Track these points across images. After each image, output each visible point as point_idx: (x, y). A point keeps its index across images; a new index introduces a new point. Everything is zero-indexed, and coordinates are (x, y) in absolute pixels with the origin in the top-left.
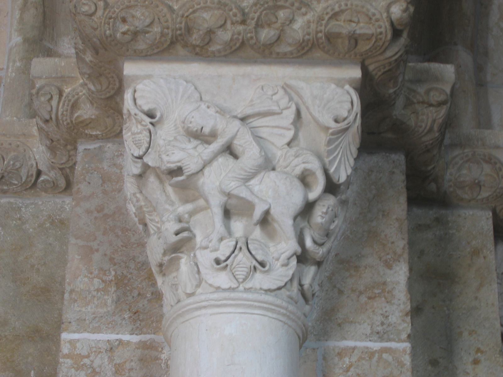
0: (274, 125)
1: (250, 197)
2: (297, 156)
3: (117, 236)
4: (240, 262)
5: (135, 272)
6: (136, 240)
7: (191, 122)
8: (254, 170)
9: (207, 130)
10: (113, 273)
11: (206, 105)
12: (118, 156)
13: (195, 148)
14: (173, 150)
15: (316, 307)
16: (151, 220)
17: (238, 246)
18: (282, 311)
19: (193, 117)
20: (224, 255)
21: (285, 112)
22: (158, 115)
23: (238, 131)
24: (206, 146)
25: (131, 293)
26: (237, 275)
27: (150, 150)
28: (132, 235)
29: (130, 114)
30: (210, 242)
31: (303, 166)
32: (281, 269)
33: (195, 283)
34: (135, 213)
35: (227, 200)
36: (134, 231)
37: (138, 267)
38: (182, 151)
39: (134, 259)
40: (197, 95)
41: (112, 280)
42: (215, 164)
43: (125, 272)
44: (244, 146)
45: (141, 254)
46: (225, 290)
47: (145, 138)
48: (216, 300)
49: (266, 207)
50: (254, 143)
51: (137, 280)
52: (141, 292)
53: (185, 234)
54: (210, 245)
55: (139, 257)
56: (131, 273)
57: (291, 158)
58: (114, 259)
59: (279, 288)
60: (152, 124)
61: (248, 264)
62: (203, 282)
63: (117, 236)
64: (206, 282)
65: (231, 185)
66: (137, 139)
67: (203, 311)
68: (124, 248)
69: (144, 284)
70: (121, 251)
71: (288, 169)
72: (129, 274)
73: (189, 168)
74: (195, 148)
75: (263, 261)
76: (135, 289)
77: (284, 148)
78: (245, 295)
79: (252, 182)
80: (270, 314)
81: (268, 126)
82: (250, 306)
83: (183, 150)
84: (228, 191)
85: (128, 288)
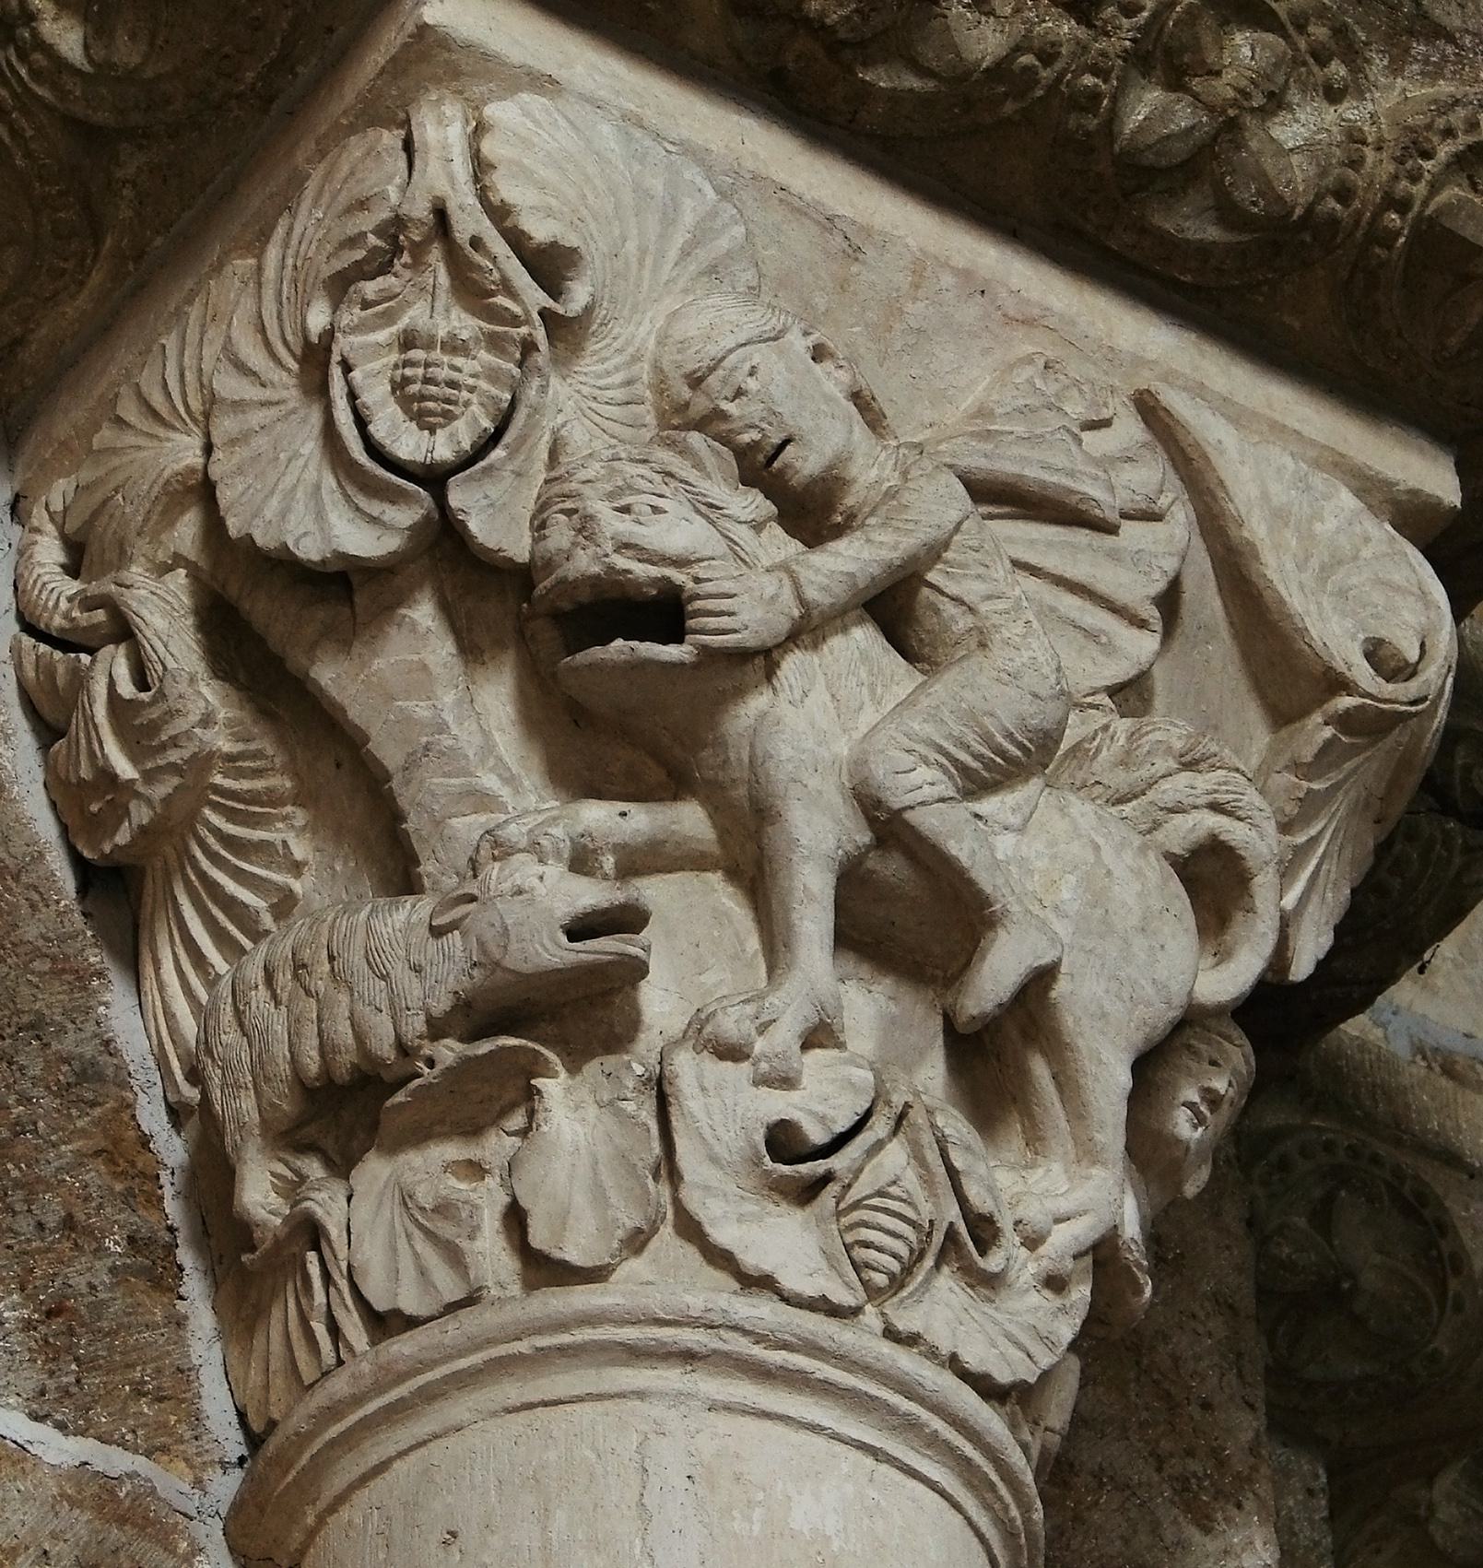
0: (1070, 572)
7: (739, 393)
8: (1020, 746)
11: (810, 341)
14: (661, 496)
20: (822, 1119)
21: (1132, 532)
25: (29, 1202)
26: (867, 1245)
27: (498, 453)
30: (762, 1029)
32: (1034, 1299)
35: (869, 848)
36: (35, 888)
38: (698, 512)
39: (37, 1026)
44: (984, 608)
47: (483, 385)
48: (759, 1339)
52: (80, 1216)
54: (759, 1046)
55: (62, 1030)
56: (25, 1100)
57: (1163, 764)
66: (443, 373)
67: (671, 1377)
71: (1127, 809)
73: (731, 614)
76: (49, 1188)
77: (1096, 707)
79: (988, 805)
82: (909, 1427)
83: (709, 510)
84: (896, 804)
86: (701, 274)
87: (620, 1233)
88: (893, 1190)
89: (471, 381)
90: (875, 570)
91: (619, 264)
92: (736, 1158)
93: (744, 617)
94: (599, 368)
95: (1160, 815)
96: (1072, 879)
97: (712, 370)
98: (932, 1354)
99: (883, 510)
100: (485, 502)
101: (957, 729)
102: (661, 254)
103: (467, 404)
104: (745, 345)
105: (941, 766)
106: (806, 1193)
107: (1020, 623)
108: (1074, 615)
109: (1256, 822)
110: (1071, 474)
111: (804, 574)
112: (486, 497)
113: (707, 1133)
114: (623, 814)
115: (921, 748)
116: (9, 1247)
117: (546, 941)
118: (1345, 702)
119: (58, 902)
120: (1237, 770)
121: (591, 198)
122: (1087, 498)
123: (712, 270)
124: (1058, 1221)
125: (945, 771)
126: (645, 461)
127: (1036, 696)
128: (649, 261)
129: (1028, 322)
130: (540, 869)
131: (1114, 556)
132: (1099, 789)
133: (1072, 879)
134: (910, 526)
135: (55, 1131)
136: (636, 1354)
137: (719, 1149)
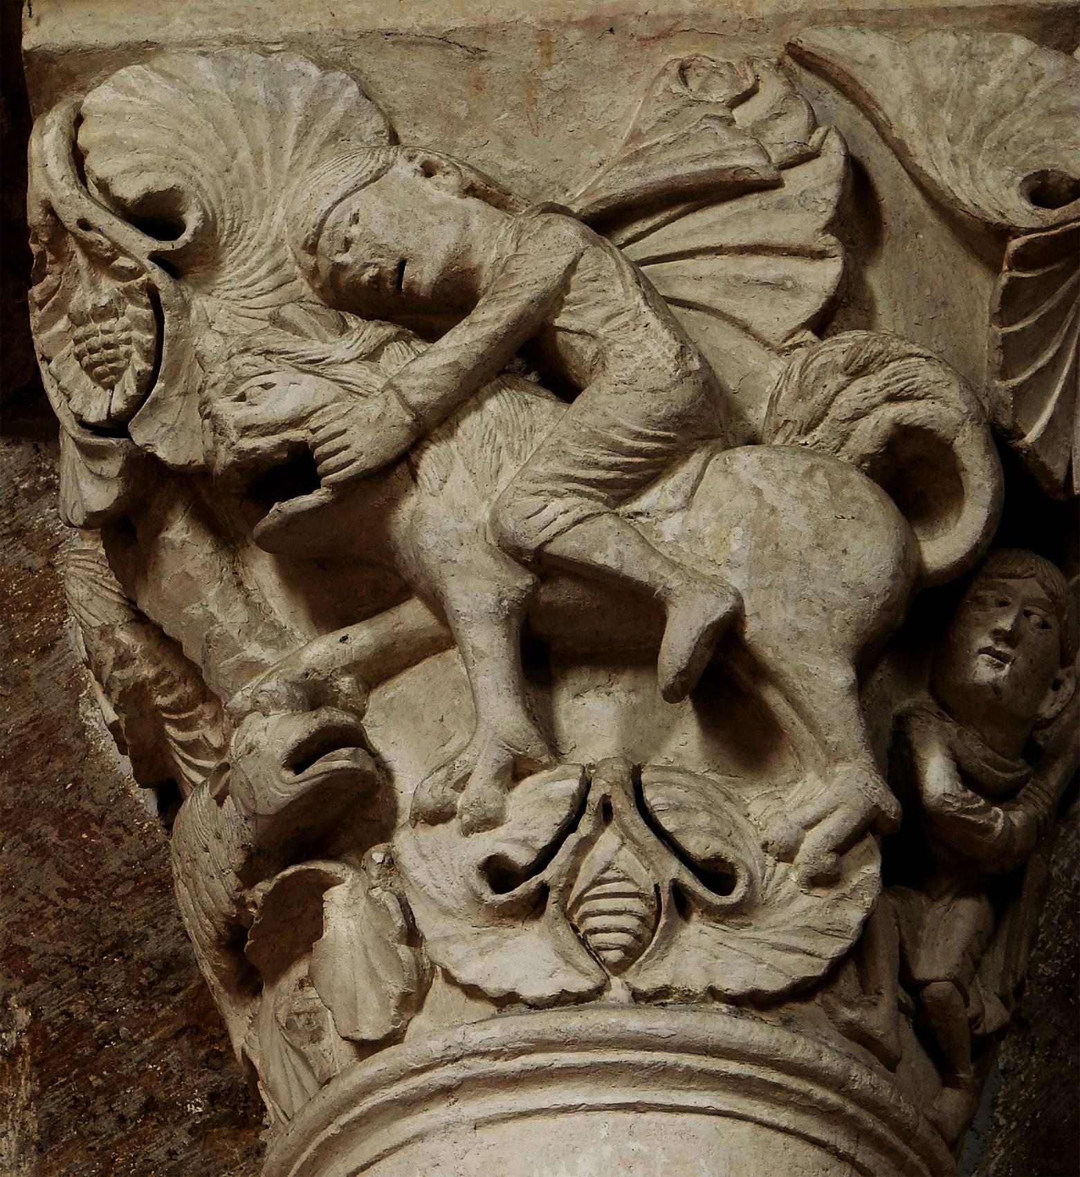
0: (746, 239)
1: (638, 568)
2: (857, 371)
3: (41, 851)
4: (606, 869)
5: (128, 1007)
6: (127, 864)
7: (348, 243)
9: (423, 274)
10: (23, 1017)
11: (416, 164)
12: (32, 495)
13: (372, 355)
14: (270, 372)
15: (1002, 1121)
16: (192, 748)
17: (594, 797)
18: (819, 1093)
19: (355, 219)
20: (524, 842)
21: (796, 179)
22: (192, 220)
23: (572, 268)
24: (420, 346)
25: (108, 1103)
26: (595, 931)
27: (159, 385)
28: (108, 844)
29: (57, 227)
30: (461, 785)
31: (891, 412)
32: (804, 901)
33: (395, 986)
34: (113, 728)
35: (535, 587)
36: (119, 823)
37: (142, 981)
39: (121, 944)
40: (372, 124)
41: (18, 1050)
42: (471, 425)
43: (79, 1010)
44: (601, 332)
45: (154, 927)
46: (538, 1005)
47: (136, 334)
48: (497, 1055)
49: (719, 609)
50: (650, 318)
51: (136, 1043)
53: (341, 760)
54: (461, 800)
55: (145, 937)
57: (832, 384)
58: (25, 951)
59: (802, 991)
60: (156, 257)
61: (645, 879)
62: (438, 983)
63: (41, 851)
64: (450, 979)
65: (547, 514)
66: (95, 341)
67: (440, 1113)
68: (73, 903)
69: (172, 1056)
70: (57, 916)
71: (817, 433)
72: (101, 1019)
73: (346, 448)
74: (372, 355)
75: (718, 860)
76: (129, 1080)
77: (799, 345)
78: (638, 1022)
79: (645, 502)
80: (761, 1110)
81: (718, 251)
82: (661, 1074)
83: (314, 366)
84: (533, 544)
85: (95, 1081)
86: (324, 144)
87: (393, 1002)
88: (606, 875)
89: (124, 335)
90: (480, 348)
91: (234, 176)
92: (463, 903)
93: (356, 446)
94: (242, 269)
95: (844, 428)
96: (738, 530)
97: (318, 234)
98: (687, 998)
99: (490, 292)
100: (164, 430)
101: (580, 453)
102: (278, 147)
103: (128, 355)
104: (341, 200)
105: (574, 491)
106: (534, 907)
107: (641, 329)
108: (759, 274)
109: (937, 393)
110: (720, 155)
111: (404, 384)
112: (164, 425)
113: (434, 892)
114: (344, 639)
115: (548, 486)
116: (92, 1149)
117: (277, 783)
118: (1015, 244)
119: (141, 826)
120: (911, 355)
121: (188, 135)
122: (738, 170)
123: (336, 136)
124: (809, 826)
125: (581, 494)
126: (247, 350)
127: (653, 391)
128: (266, 158)
129: (664, 35)
130: (264, 721)
131: (782, 206)
132: (790, 426)
133: (738, 530)
134: (514, 292)
135: (136, 1030)
136: (409, 1104)
137: (449, 902)
